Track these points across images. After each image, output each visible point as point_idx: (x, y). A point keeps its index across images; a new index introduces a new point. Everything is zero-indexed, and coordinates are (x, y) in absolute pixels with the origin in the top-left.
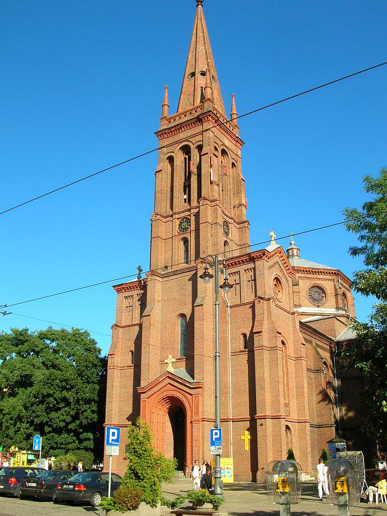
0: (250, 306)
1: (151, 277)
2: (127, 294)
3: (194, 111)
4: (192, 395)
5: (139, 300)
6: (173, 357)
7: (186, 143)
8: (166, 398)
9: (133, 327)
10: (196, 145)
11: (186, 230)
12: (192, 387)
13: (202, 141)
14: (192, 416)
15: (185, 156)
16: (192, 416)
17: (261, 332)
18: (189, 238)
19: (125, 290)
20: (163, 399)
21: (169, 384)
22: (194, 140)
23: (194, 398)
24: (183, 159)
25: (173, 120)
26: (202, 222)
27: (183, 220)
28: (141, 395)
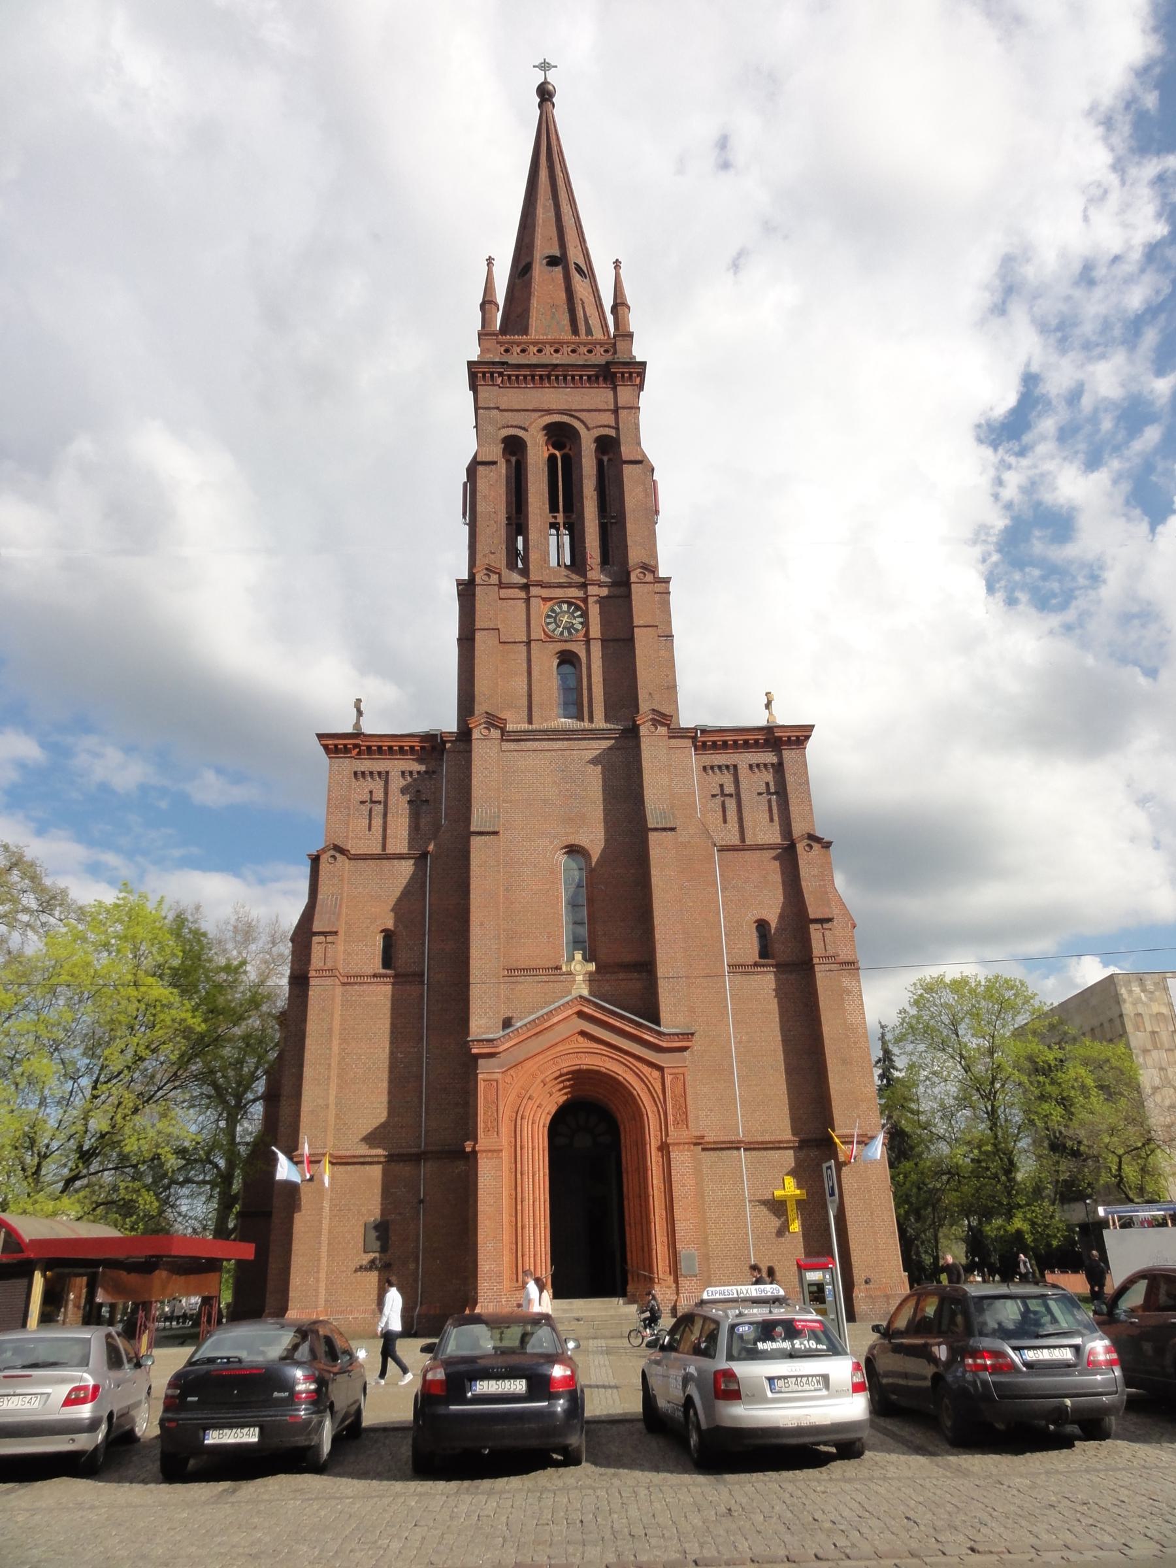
0: (774, 853)
1: (485, 732)
2: (366, 765)
3: (584, 350)
4: (660, 1069)
5: (403, 791)
6: (586, 959)
7: (565, 419)
8: (567, 1074)
9: (396, 862)
10: (597, 432)
11: (570, 633)
12: (664, 1044)
13: (617, 429)
14: (664, 1128)
15: (553, 451)
16: (664, 1128)
17: (829, 920)
18: (583, 655)
19: (359, 753)
20: (561, 1075)
21: (583, 1033)
22: (592, 419)
23: (668, 1078)
24: (546, 455)
25: (535, 349)
26: (641, 623)
27: (560, 608)
28: (481, 1062)
